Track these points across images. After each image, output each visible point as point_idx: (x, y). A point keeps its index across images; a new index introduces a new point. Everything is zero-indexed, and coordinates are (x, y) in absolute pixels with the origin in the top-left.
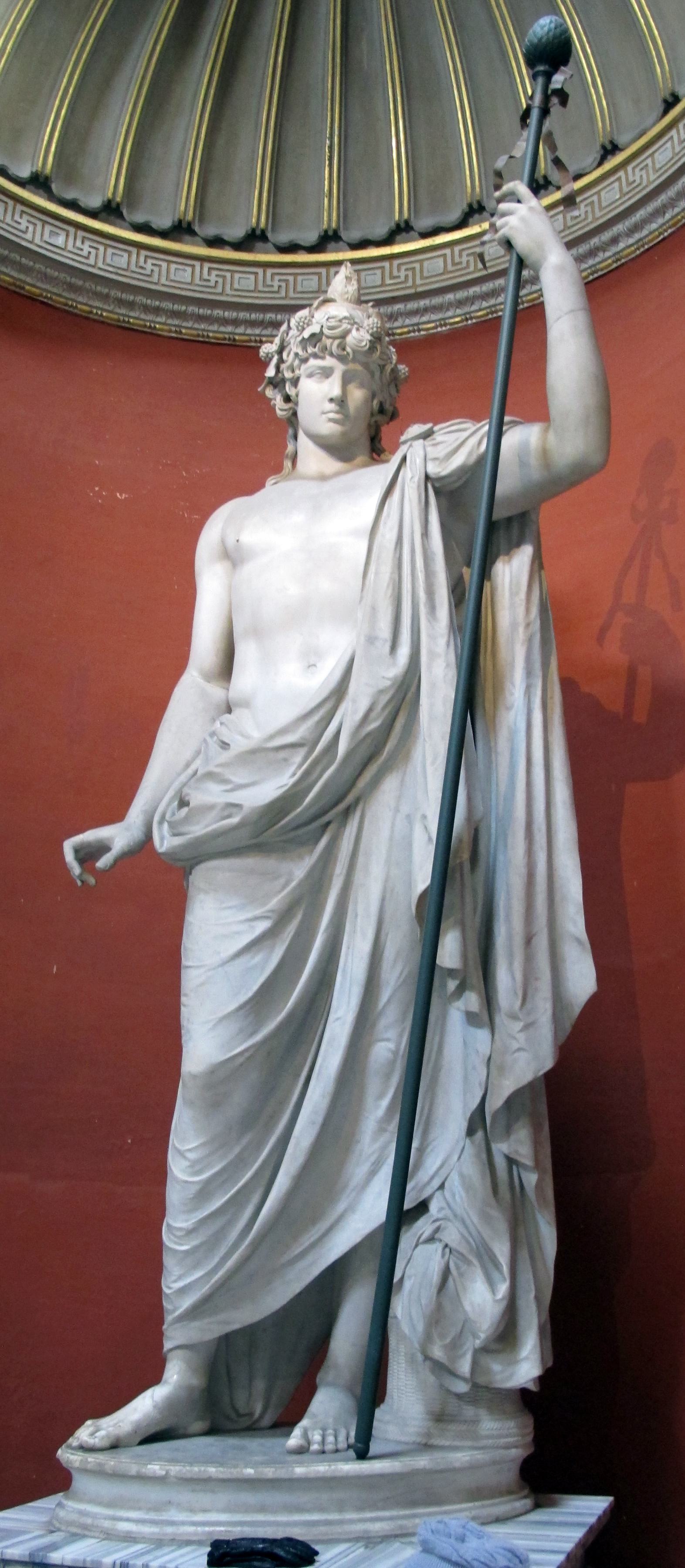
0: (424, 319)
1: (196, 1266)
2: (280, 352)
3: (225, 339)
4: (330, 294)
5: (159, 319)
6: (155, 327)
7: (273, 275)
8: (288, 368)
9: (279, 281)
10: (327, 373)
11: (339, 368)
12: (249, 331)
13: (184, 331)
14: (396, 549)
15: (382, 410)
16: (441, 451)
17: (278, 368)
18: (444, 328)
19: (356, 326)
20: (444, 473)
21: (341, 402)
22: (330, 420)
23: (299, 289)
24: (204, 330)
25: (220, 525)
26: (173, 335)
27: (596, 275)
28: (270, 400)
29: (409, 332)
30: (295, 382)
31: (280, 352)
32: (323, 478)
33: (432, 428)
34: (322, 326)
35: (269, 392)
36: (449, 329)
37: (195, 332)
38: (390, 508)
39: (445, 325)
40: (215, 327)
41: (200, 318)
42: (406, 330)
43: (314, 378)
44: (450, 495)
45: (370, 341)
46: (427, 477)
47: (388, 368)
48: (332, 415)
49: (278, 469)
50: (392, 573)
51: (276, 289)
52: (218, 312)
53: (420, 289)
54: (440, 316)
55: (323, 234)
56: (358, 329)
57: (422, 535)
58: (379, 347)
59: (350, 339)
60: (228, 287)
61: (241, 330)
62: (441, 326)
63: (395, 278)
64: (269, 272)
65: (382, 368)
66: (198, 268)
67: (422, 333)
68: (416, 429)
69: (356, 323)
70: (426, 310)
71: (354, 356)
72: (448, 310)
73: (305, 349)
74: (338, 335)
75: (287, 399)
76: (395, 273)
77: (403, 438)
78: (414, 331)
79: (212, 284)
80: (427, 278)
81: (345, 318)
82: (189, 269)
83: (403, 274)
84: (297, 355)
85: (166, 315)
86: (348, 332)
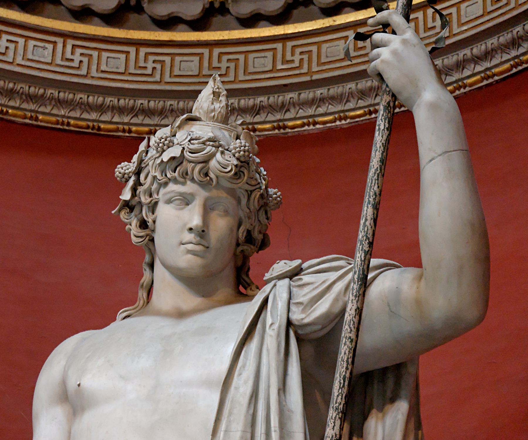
0: (321, 110)
2: (138, 173)
3: (88, 127)
4: (195, 113)
5: (12, 103)
6: (7, 112)
7: (147, 54)
9: (154, 62)
10: (186, 200)
11: (201, 195)
12: (116, 119)
13: (40, 117)
14: (250, 403)
15: (249, 239)
16: (303, 295)
17: (134, 190)
18: (343, 122)
19: (220, 149)
20: (306, 321)
21: (202, 233)
22: (189, 252)
23: (176, 72)
24: (63, 116)
25: (63, 363)
26: (27, 121)
27: (520, 68)
28: (126, 224)
29: (303, 125)
30: (153, 207)
31: (138, 173)
32: (181, 315)
33: (301, 265)
34: (184, 148)
35: (123, 215)
36: (349, 123)
37: (54, 119)
38: (246, 358)
39: (345, 118)
40: (76, 114)
41: (60, 103)
42: (299, 122)
43: (172, 205)
44: (314, 344)
45: (236, 166)
46: (289, 323)
47: (257, 195)
48: (190, 247)
49: (132, 302)
50: (244, 431)
51: (149, 71)
52: (81, 96)
53: (315, 77)
54: (340, 108)
55: (207, 6)
56: (222, 153)
57: (279, 390)
58: (246, 172)
59: (213, 163)
60: (94, 67)
61: (106, 117)
62: (340, 119)
63: (288, 62)
64: (143, 51)
65: (250, 194)
66: (60, 46)
67: (318, 126)
68: (282, 266)
69: (220, 146)
70: (322, 100)
71: (218, 182)
72: (348, 101)
73: (163, 172)
74: (201, 159)
75: (143, 224)
76: (289, 57)
77: (267, 276)
78: (309, 124)
79: (76, 64)
80: (324, 64)
81: (209, 140)
82: (50, 47)
83: (297, 58)
84: (155, 177)
85: (21, 98)
86: (212, 156)
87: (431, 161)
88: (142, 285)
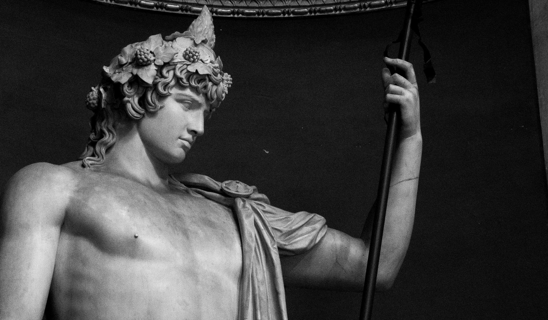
8: (164, 83)
10: (192, 105)
11: (204, 107)
22: (184, 147)
30: (162, 97)
43: (182, 105)
48: (187, 144)
87: (409, 179)
88: (107, 144)
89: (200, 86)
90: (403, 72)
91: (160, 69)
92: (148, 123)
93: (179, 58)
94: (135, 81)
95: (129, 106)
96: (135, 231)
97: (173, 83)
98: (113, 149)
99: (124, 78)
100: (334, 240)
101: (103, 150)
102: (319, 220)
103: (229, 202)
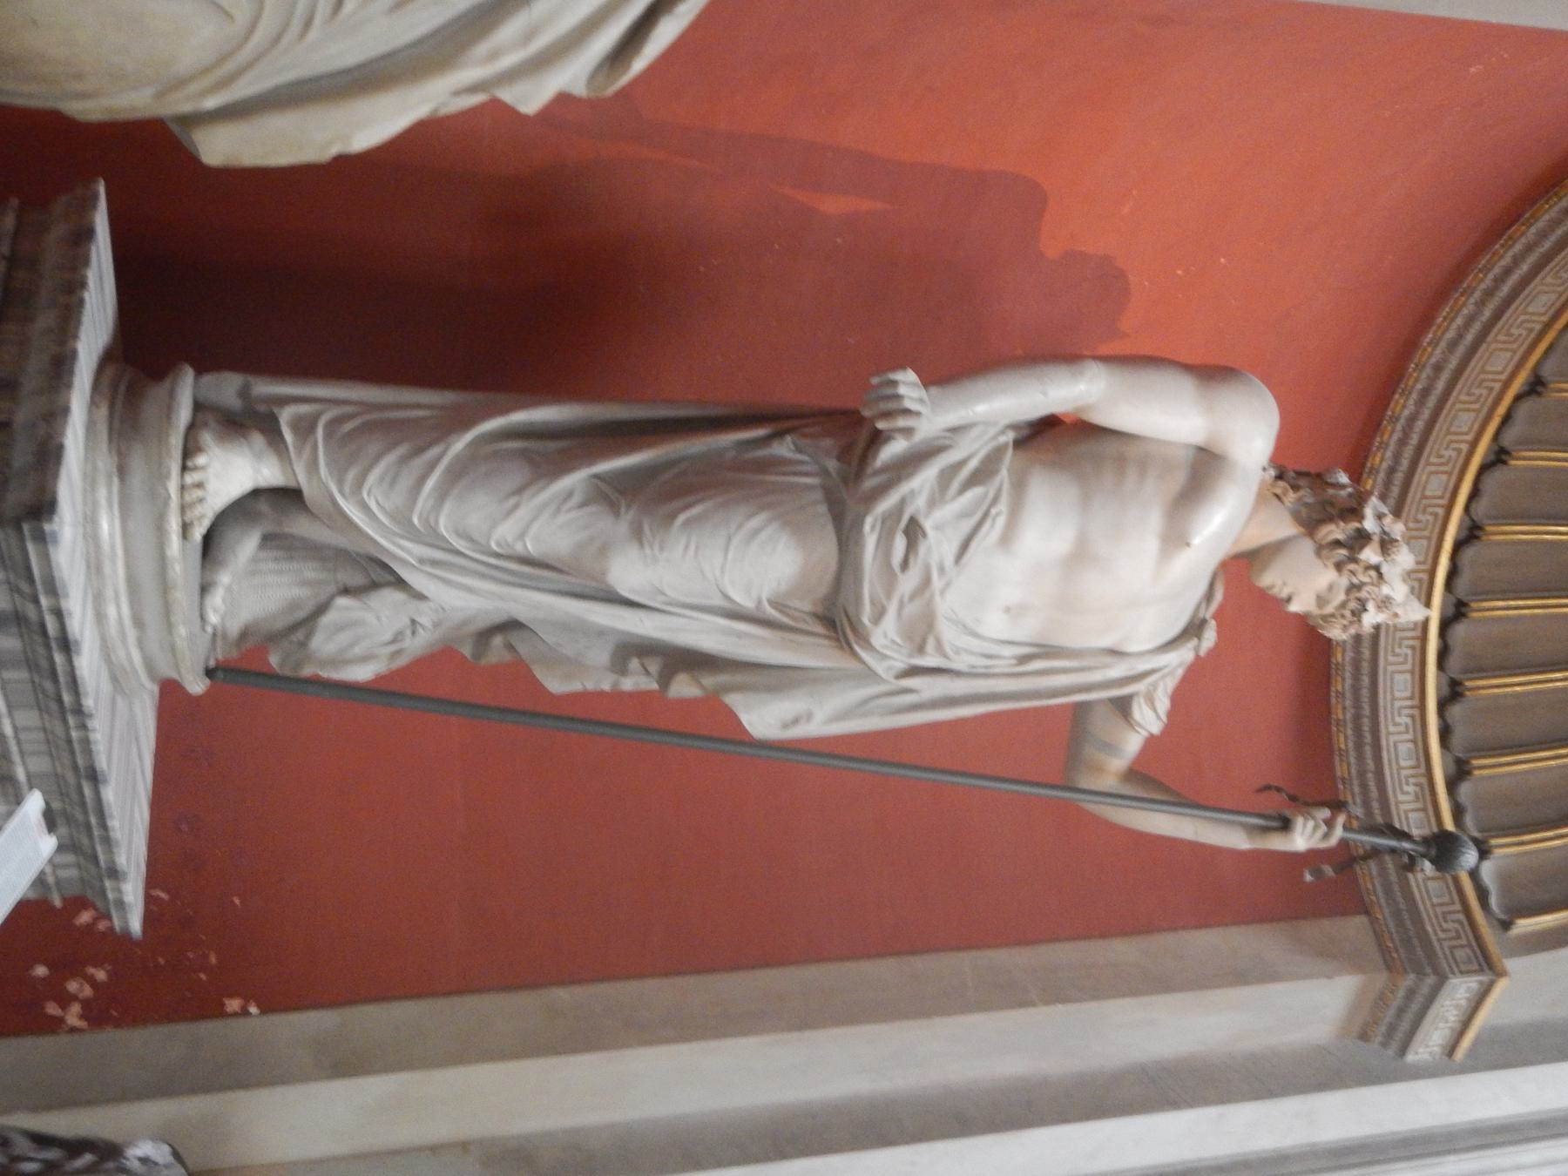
1: (392, 516)
10: (1321, 600)
22: (1272, 587)
30: (1339, 566)
54: (1443, 344)
70: (1460, 336)
89: (1347, 613)
90: (1326, 836)
91: (1377, 568)
92: (1307, 546)
93: (1385, 590)
94: (1362, 538)
95: (1332, 527)
96: (1196, 541)
97: (1355, 581)
98: (1275, 501)
99: (1369, 524)
100: (1132, 744)
101: (1278, 491)
102: (1155, 727)
103: (1194, 629)
